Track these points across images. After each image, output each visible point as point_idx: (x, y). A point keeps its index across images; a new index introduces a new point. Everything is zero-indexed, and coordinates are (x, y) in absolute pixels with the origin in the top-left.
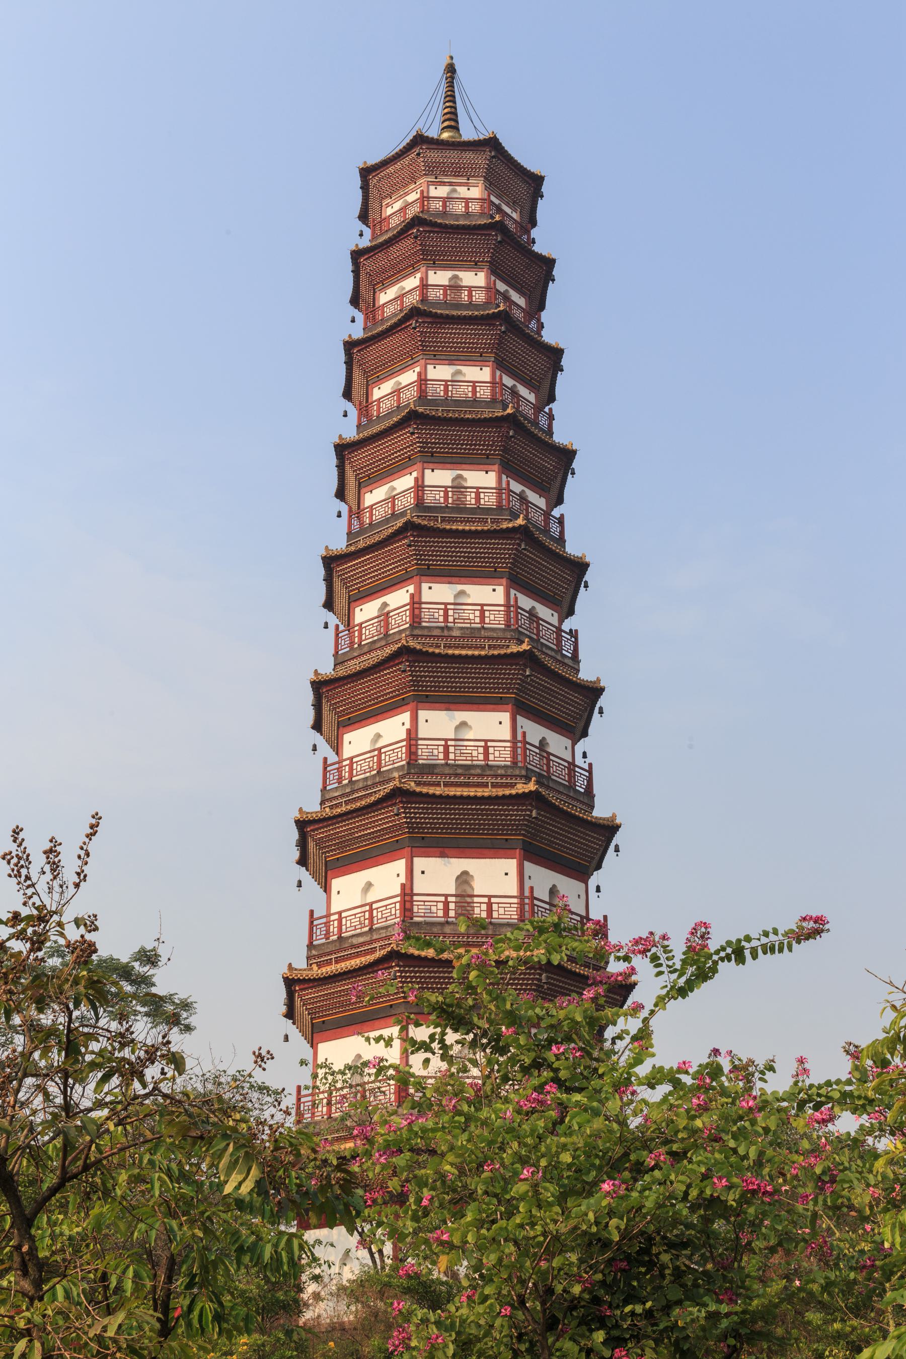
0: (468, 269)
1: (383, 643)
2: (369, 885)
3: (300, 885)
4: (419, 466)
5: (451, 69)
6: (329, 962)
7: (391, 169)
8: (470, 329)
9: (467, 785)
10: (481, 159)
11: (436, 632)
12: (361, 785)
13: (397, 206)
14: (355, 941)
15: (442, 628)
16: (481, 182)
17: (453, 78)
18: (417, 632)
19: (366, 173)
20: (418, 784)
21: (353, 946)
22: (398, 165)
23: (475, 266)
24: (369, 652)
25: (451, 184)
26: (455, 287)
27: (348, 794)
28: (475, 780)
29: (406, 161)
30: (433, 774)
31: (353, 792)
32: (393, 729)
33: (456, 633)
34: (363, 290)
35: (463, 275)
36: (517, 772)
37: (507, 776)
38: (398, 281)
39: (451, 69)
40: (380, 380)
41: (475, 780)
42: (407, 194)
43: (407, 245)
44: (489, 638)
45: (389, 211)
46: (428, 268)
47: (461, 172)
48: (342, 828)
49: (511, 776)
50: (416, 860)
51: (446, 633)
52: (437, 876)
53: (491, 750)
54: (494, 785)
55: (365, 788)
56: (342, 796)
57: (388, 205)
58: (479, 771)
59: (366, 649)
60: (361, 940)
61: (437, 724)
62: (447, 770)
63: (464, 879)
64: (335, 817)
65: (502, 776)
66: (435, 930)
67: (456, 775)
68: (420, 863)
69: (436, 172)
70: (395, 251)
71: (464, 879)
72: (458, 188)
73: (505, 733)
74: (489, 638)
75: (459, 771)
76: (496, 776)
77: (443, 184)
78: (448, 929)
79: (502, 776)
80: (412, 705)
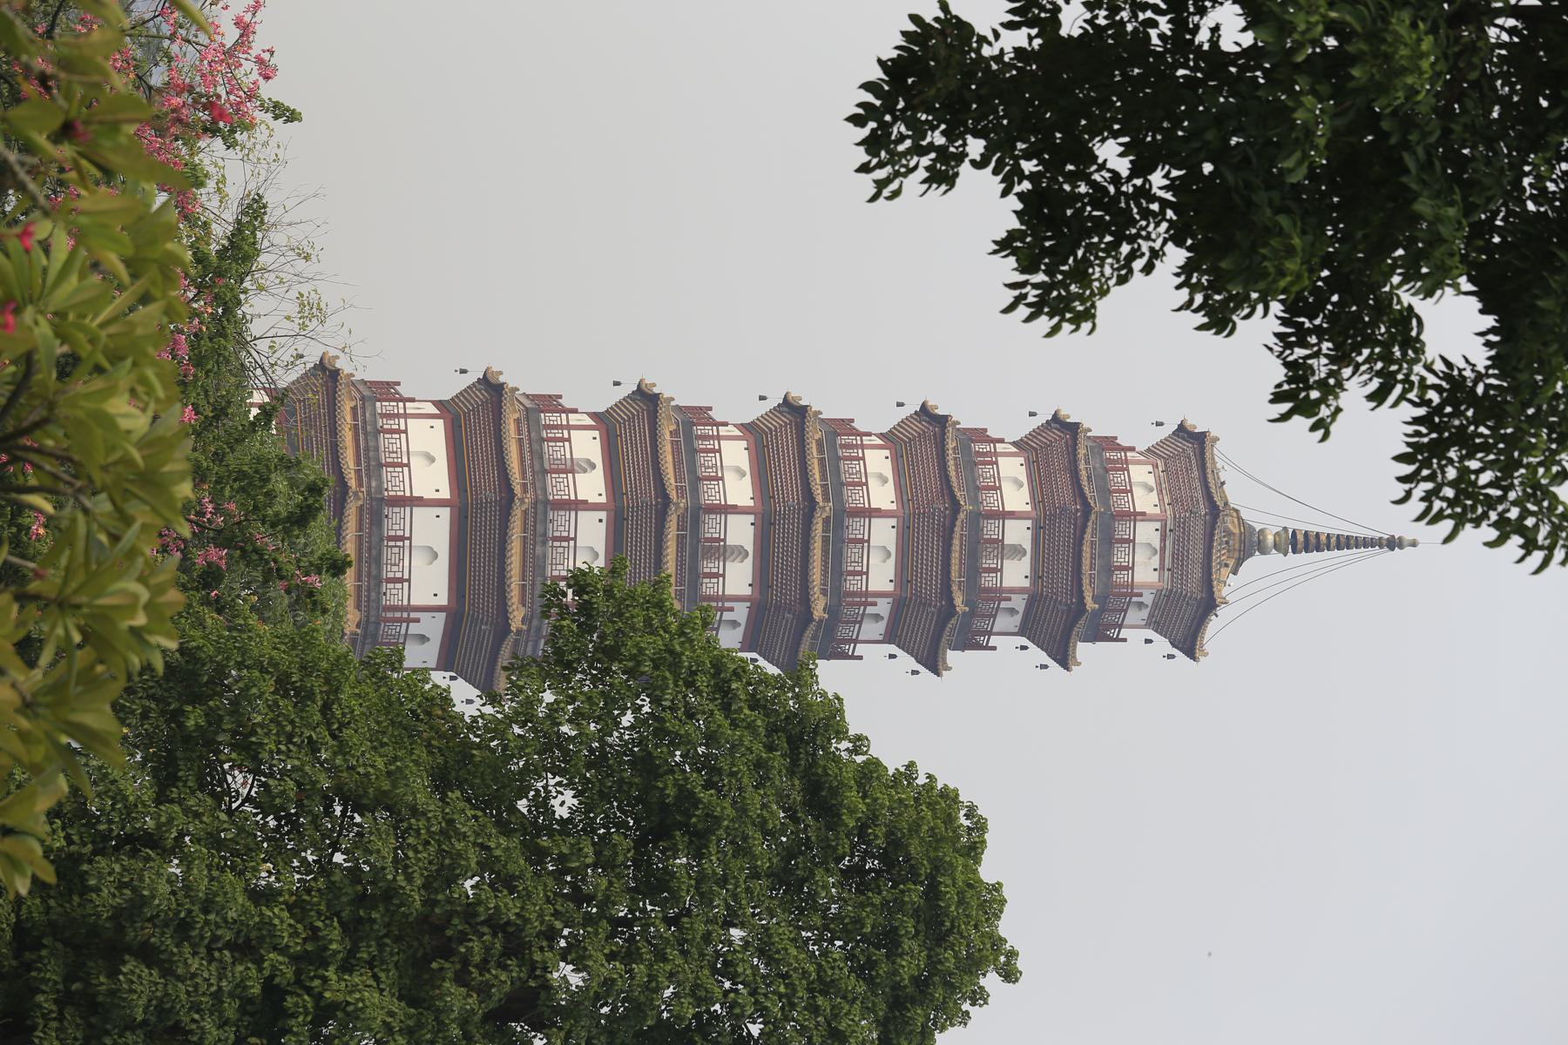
1: (537, 468)
7: (1196, 473)
8: (937, 570)
11: (540, 528)
12: (371, 444)
15: (545, 534)
16: (1166, 585)
17: (1381, 547)
18: (540, 507)
20: (361, 509)
22: (1197, 484)
23: (1036, 575)
24: (531, 452)
25: (1163, 549)
27: (364, 428)
29: (1199, 495)
30: (371, 524)
31: (366, 434)
33: (539, 550)
36: (373, 612)
42: (1160, 492)
43: (1064, 494)
46: (1036, 522)
49: (368, 607)
51: (539, 539)
53: (399, 586)
55: (367, 449)
56: (364, 422)
58: (374, 572)
59: (536, 447)
62: (375, 539)
65: (368, 597)
67: (370, 549)
70: (1063, 480)
72: (1157, 557)
75: (374, 552)
76: (368, 591)
79: (368, 597)
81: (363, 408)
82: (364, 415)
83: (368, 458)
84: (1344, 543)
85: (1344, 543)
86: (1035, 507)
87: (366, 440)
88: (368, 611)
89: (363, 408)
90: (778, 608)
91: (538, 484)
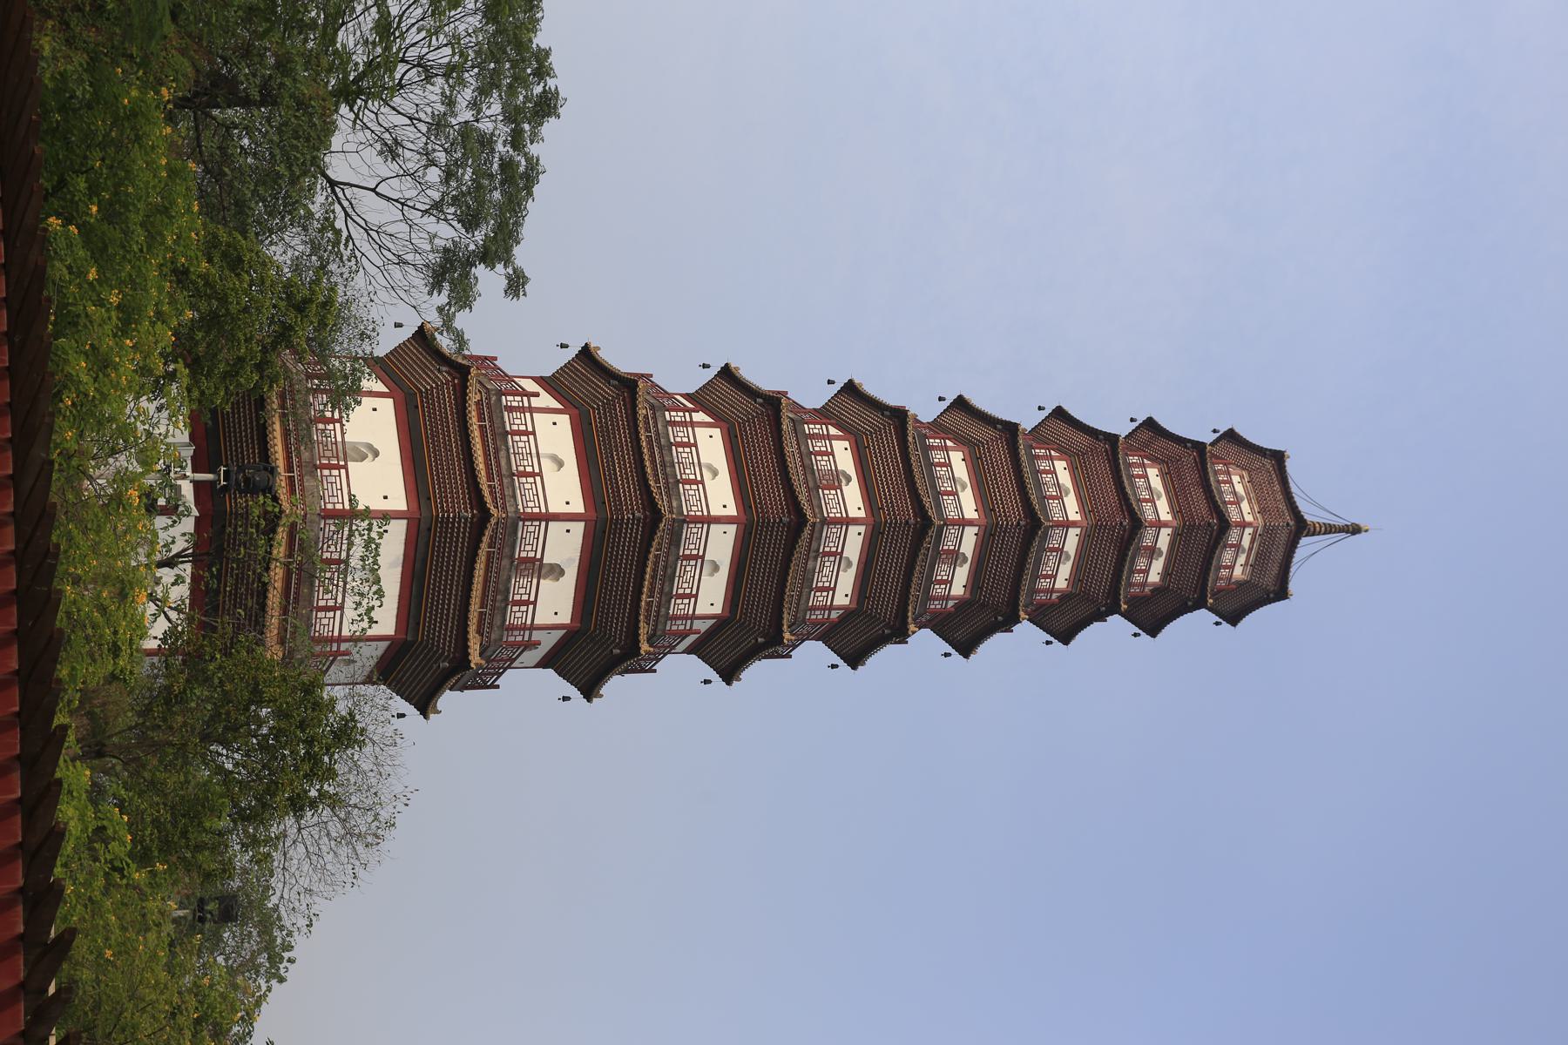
0: (1166, 568)
2: (560, 464)
3: (563, 346)
4: (984, 522)
5: (1355, 530)
6: (481, 418)
9: (654, 577)
10: (1269, 580)
11: (814, 545)
12: (667, 459)
13: (1239, 489)
14: (502, 454)
19: (1278, 457)
21: (497, 451)
22: (1280, 496)
23: (1166, 573)
24: (803, 465)
25: (1250, 549)
26: (1153, 552)
28: (658, 586)
29: (1283, 507)
30: (670, 544)
31: (660, 447)
32: (720, 496)
34: (1162, 443)
35: (1160, 533)
37: (657, 616)
38: (1167, 492)
39: (1355, 530)
40: (1072, 469)
41: (658, 586)
42: (1250, 502)
43: (1201, 508)
44: (800, 596)
45: (1236, 479)
47: (1259, 562)
48: (623, 436)
49: (656, 621)
50: (582, 524)
52: (564, 546)
54: (649, 604)
57: (1242, 477)
59: (807, 462)
60: (503, 462)
61: (721, 545)
63: (557, 571)
64: (635, 419)
65: (658, 612)
66: (506, 550)
67: (665, 567)
68: (578, 528)
69: (1265, 537)
70: (1197, 494)
71: (557, 571)
73: (702, 609)
74: (800, 596)
75: (669, 571)
76: (659, 607)
77: (1252, 542)
78: (505, 562)
79: (658, 612)
80: (744, 518)
81: (654, 418)
82: (656, 425)
83: (665, 474)
84: (1330, 529)
85: (1330, 529)
86: (1174, 517)
87: (661, 453)
88: (656, 626)
89: (654, 418)
90: (983, 606)
91: (815, 502)
